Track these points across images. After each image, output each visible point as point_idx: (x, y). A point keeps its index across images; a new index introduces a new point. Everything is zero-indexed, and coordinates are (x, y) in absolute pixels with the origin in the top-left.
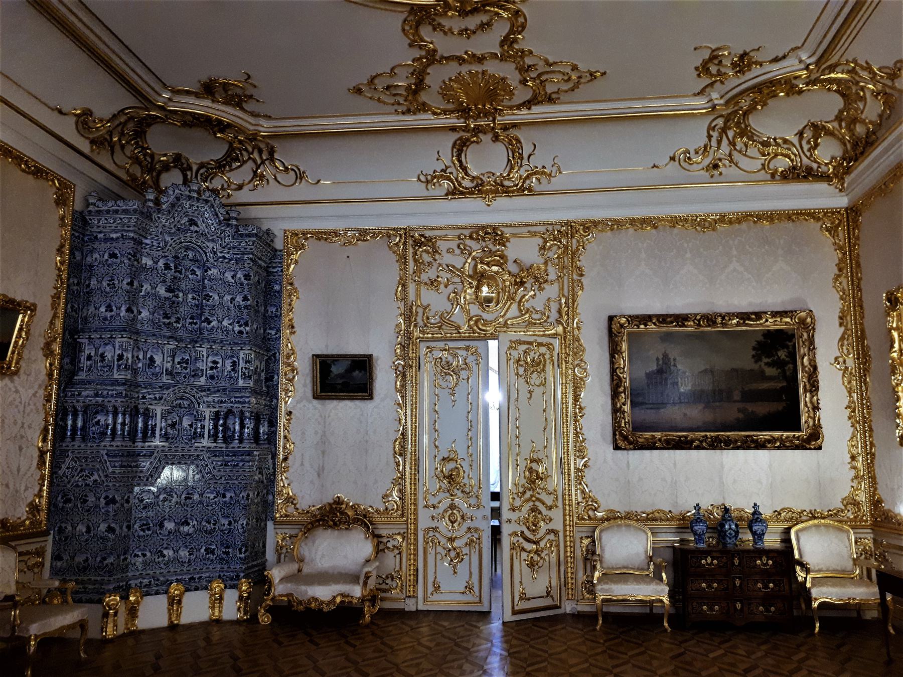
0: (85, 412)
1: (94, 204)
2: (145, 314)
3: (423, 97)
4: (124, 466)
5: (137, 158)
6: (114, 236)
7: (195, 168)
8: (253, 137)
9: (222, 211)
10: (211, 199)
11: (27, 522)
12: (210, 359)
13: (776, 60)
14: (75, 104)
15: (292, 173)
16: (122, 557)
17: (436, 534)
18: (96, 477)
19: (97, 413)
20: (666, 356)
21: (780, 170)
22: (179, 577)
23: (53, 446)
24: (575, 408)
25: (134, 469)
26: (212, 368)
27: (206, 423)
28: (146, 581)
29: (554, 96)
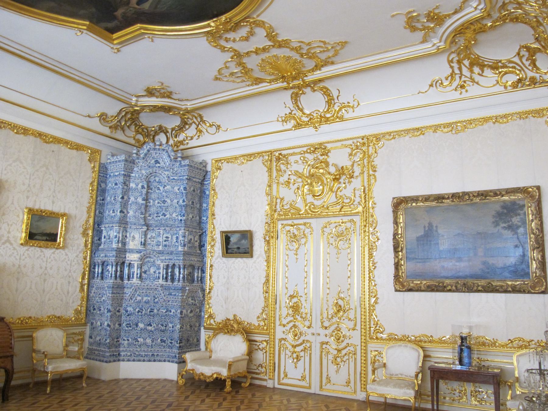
0: (103, 264)
1: (109, 159)
2: (131, 213)
4: (114, 293)
5: (138, 131)
6: (117, 174)
7: (170, 131)
8: (188, 112)
9: (173, 154)
10: (167, 148)
11: (73, 319)
12: (165, 236)
14: (96, 111)
15: (214, 126)
16: (116, 340)
17: (286, 342)
18: (104, 298)
19: (107, 265)
20: (430, 225)
21: (510, 83)
22: (146, 354)
23: (89, 282)
24: (369, 262)
25: (121, 295)
26: (165, 241)
27: (161, 271)
28: (129, 354)
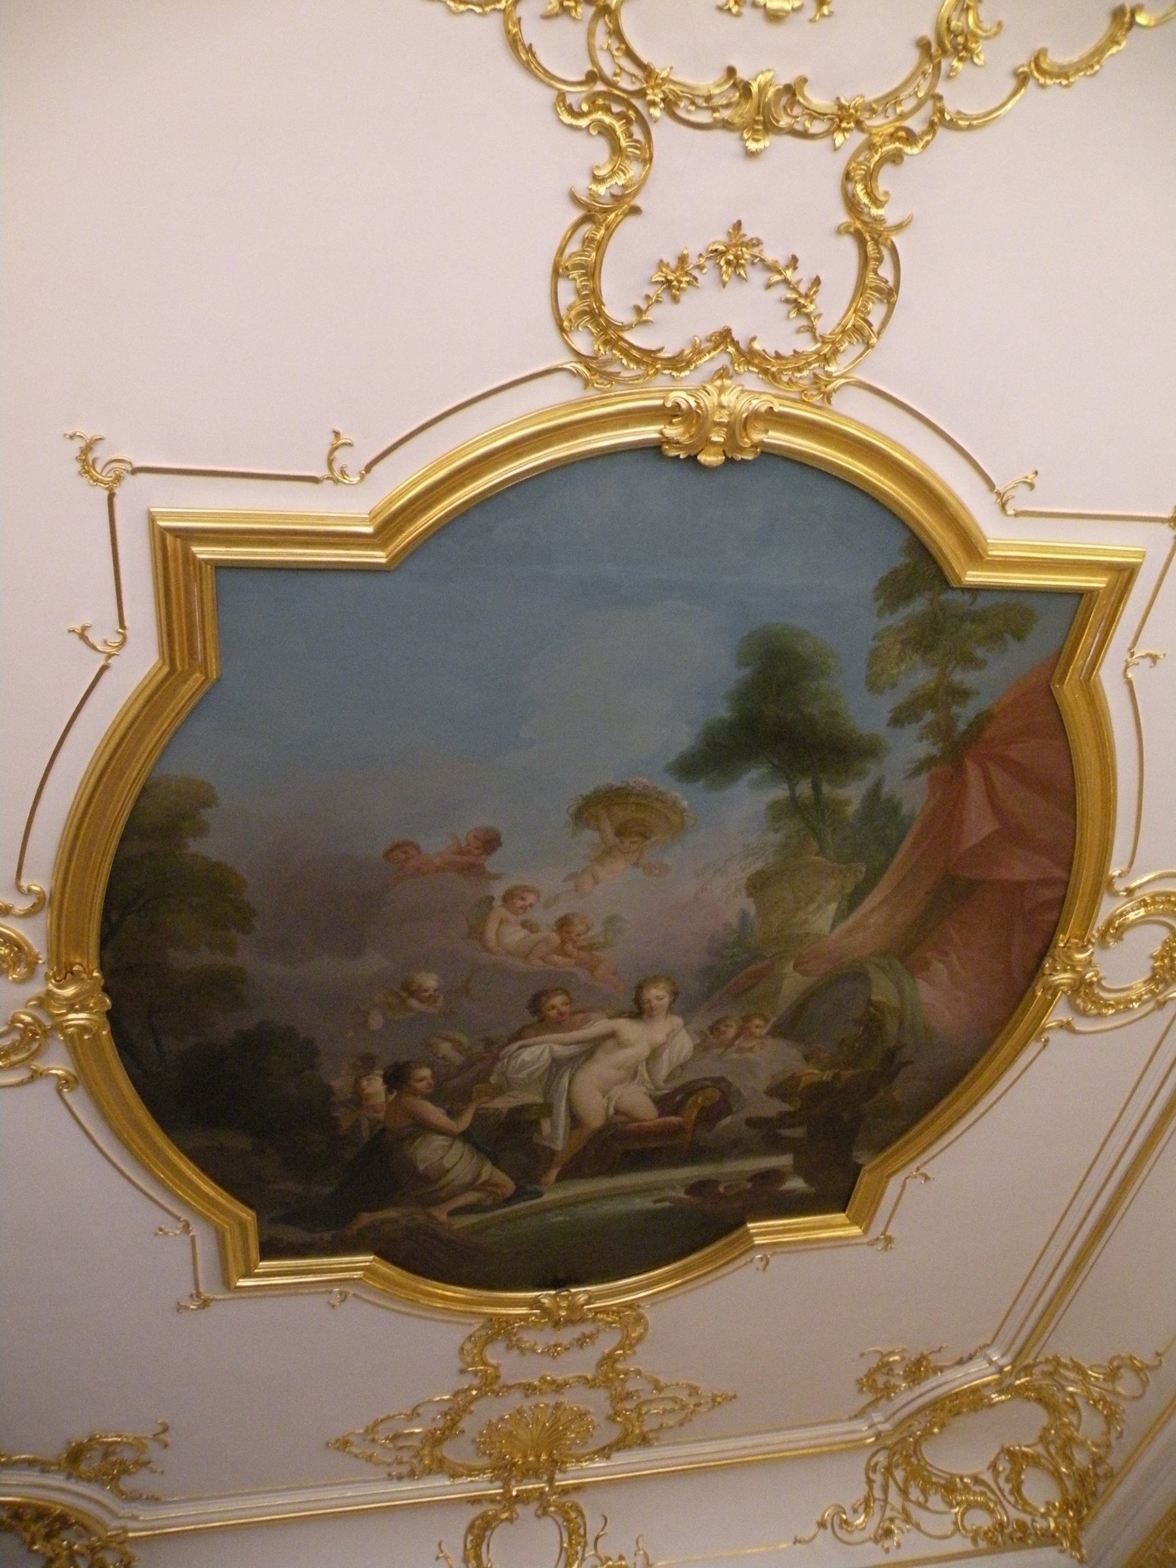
3: (448, 1451)
13: (961, 1362)
29: (651, 1435)
